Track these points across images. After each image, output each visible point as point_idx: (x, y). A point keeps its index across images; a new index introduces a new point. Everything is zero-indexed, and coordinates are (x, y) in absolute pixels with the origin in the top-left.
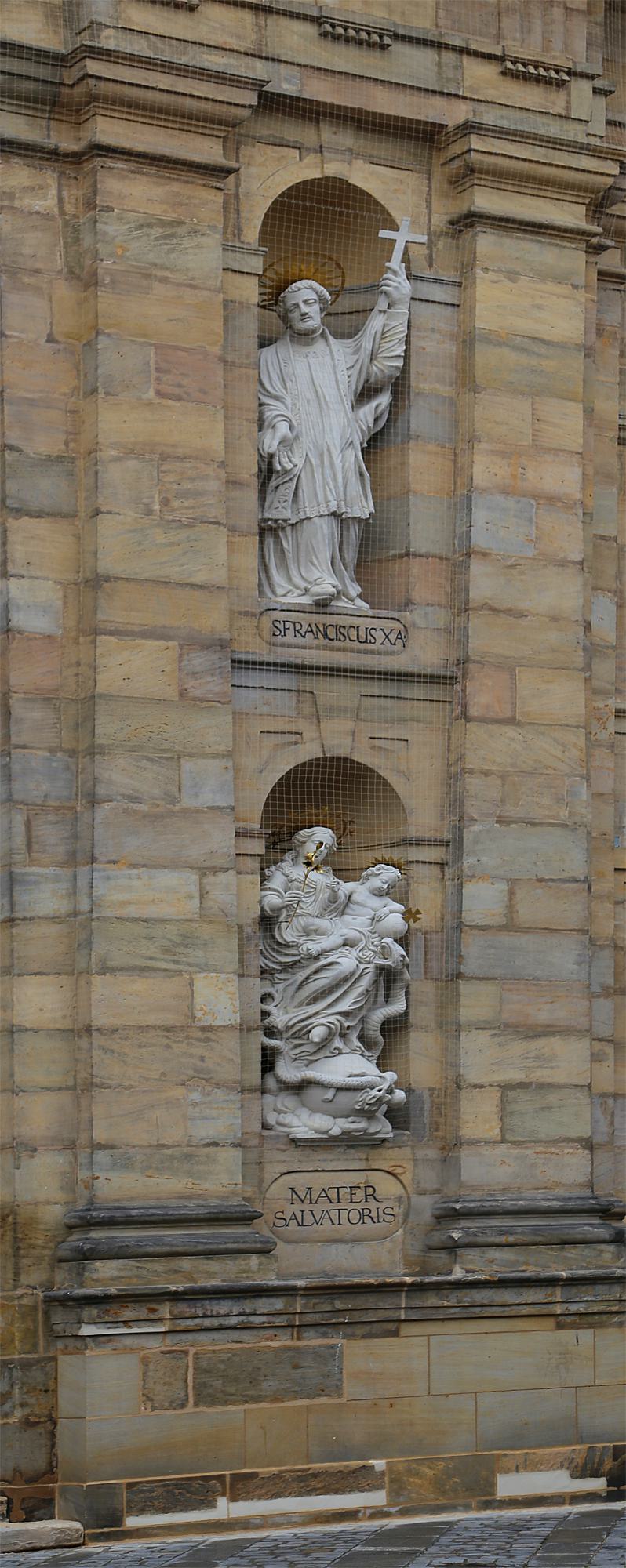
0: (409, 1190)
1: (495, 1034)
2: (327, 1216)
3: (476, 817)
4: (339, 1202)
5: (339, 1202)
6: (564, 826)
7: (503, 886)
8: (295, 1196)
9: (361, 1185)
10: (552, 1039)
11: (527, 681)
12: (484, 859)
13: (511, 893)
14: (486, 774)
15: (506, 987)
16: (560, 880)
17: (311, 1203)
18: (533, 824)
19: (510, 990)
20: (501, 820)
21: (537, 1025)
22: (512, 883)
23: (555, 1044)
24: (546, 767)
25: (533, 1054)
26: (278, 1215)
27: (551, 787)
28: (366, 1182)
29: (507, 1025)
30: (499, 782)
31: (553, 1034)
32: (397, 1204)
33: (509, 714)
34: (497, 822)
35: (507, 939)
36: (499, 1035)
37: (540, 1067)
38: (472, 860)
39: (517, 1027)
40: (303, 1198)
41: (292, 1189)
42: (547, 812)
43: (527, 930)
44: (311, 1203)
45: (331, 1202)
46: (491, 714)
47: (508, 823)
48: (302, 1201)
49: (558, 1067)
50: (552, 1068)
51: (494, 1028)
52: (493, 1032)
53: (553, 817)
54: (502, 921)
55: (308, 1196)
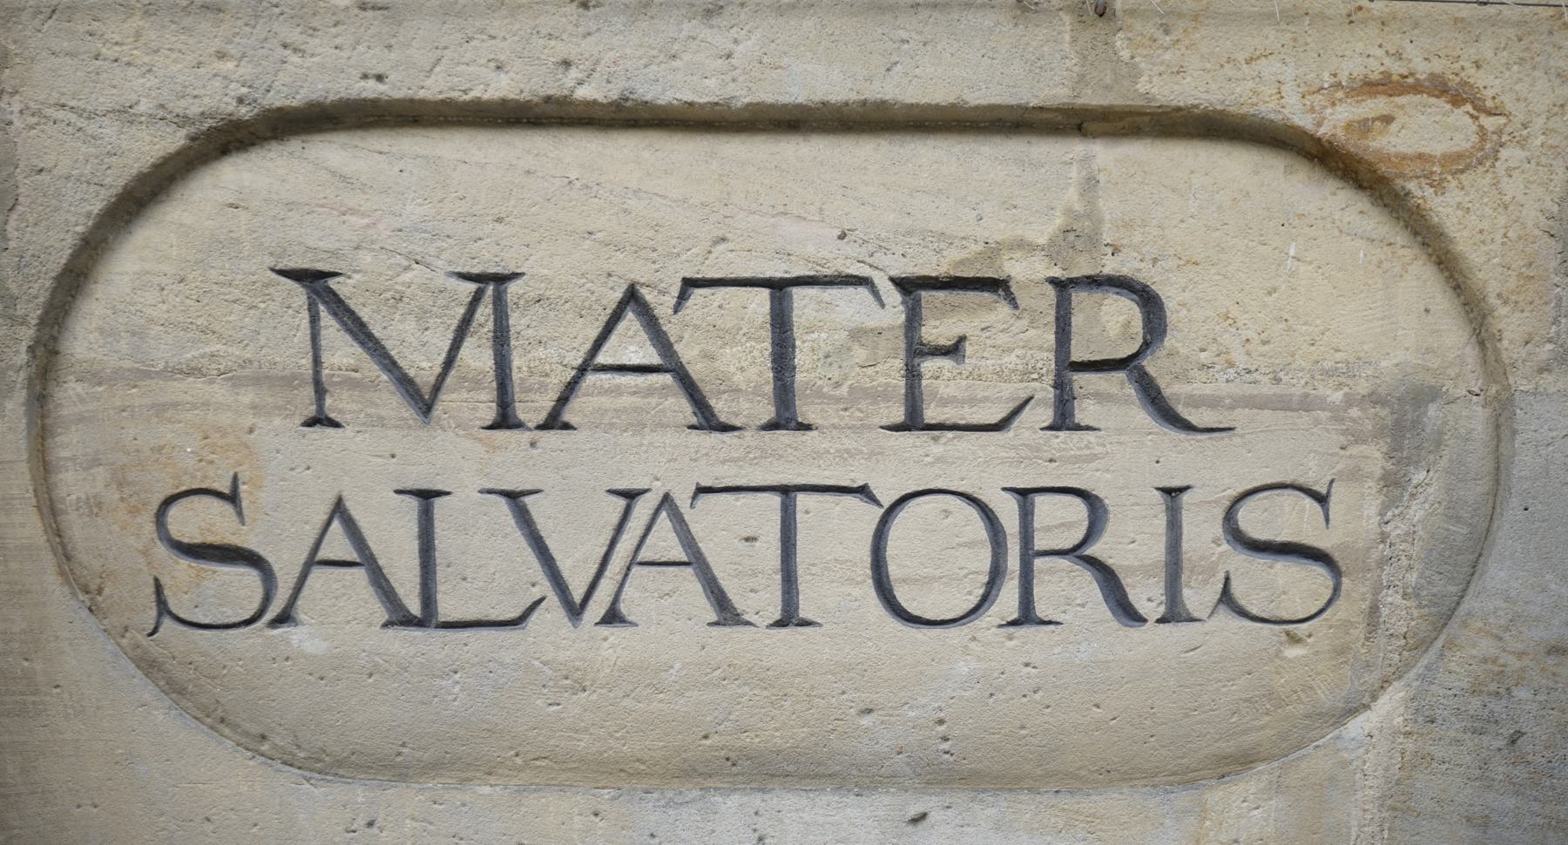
0: (1511, 325)
2: (665, 542)
4: (785, 419)
5: (785, 419)
8: (341, 352)
9: (1017, 269)
17: (505, 420)
26: (193, 520)
28: (1072, 236)
32: (1374, 457)
40: (423, 365)
41: (313, 280)
44: (505, 420)
45: (708, 421)
48: (423, 401)
55: (477, 356)
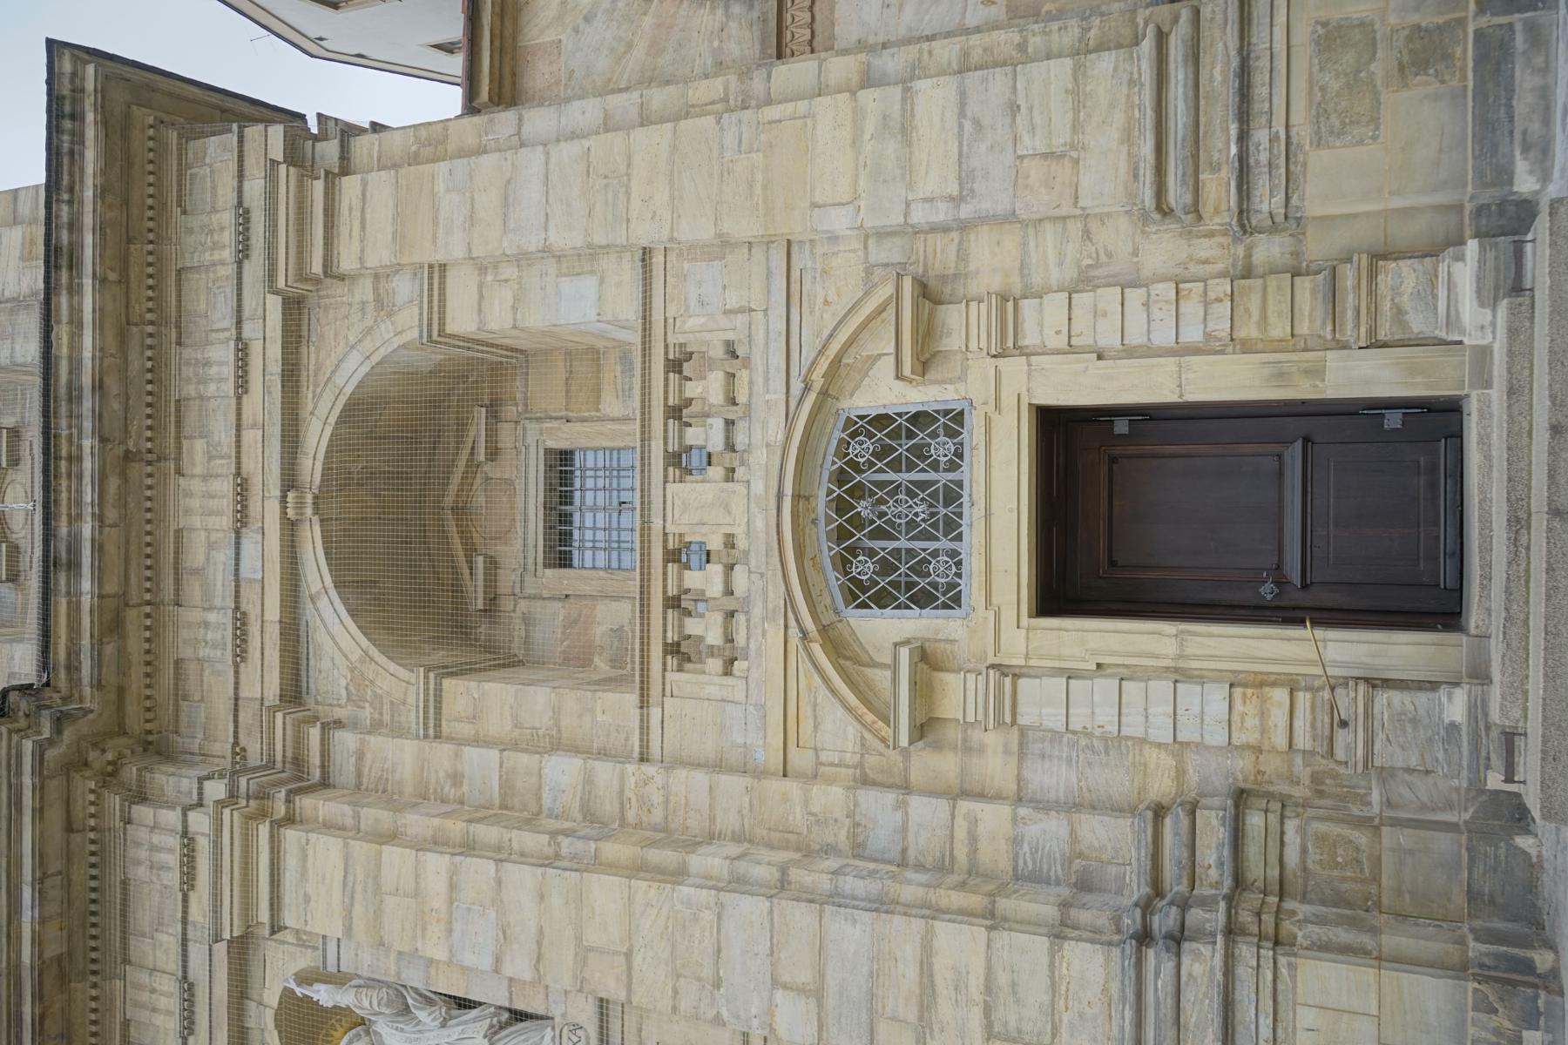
1: (931, 1034)
3: (715, 1012)
6: (719, 916)
7: (779, 994)
10: (936, 967)
11: (593, 937)
12: (754, 1010)
13: (785, 987)
14: (675, 992)
15: (880, 1011)
16: (771, 931)
18: (719, 951)
19: (884, 1007)
20: (717, 984)
21: (921, 983)
22: (776, 983)
23: (941, 964)
24: (667, 928)
25: (953, 993)
27: (684, 926)
29: (921, 1018)
30: (682, 980)
31: (931, 965)
33: (622, 959)
34: (718, 989)
35: (831, 1000)
36: (932, 1030)
37: (966, 987)
38: (755, 1023)
39: (922, 1006)
42: (707, 934)
43: (821, 975)
46: (624, 978)
47: (720, 979)
49: (966, 966)
50: (968, 973)
51: (924, 1033)
52: (928, 1036)
53: (712, 927)
54: (812, 1001)
